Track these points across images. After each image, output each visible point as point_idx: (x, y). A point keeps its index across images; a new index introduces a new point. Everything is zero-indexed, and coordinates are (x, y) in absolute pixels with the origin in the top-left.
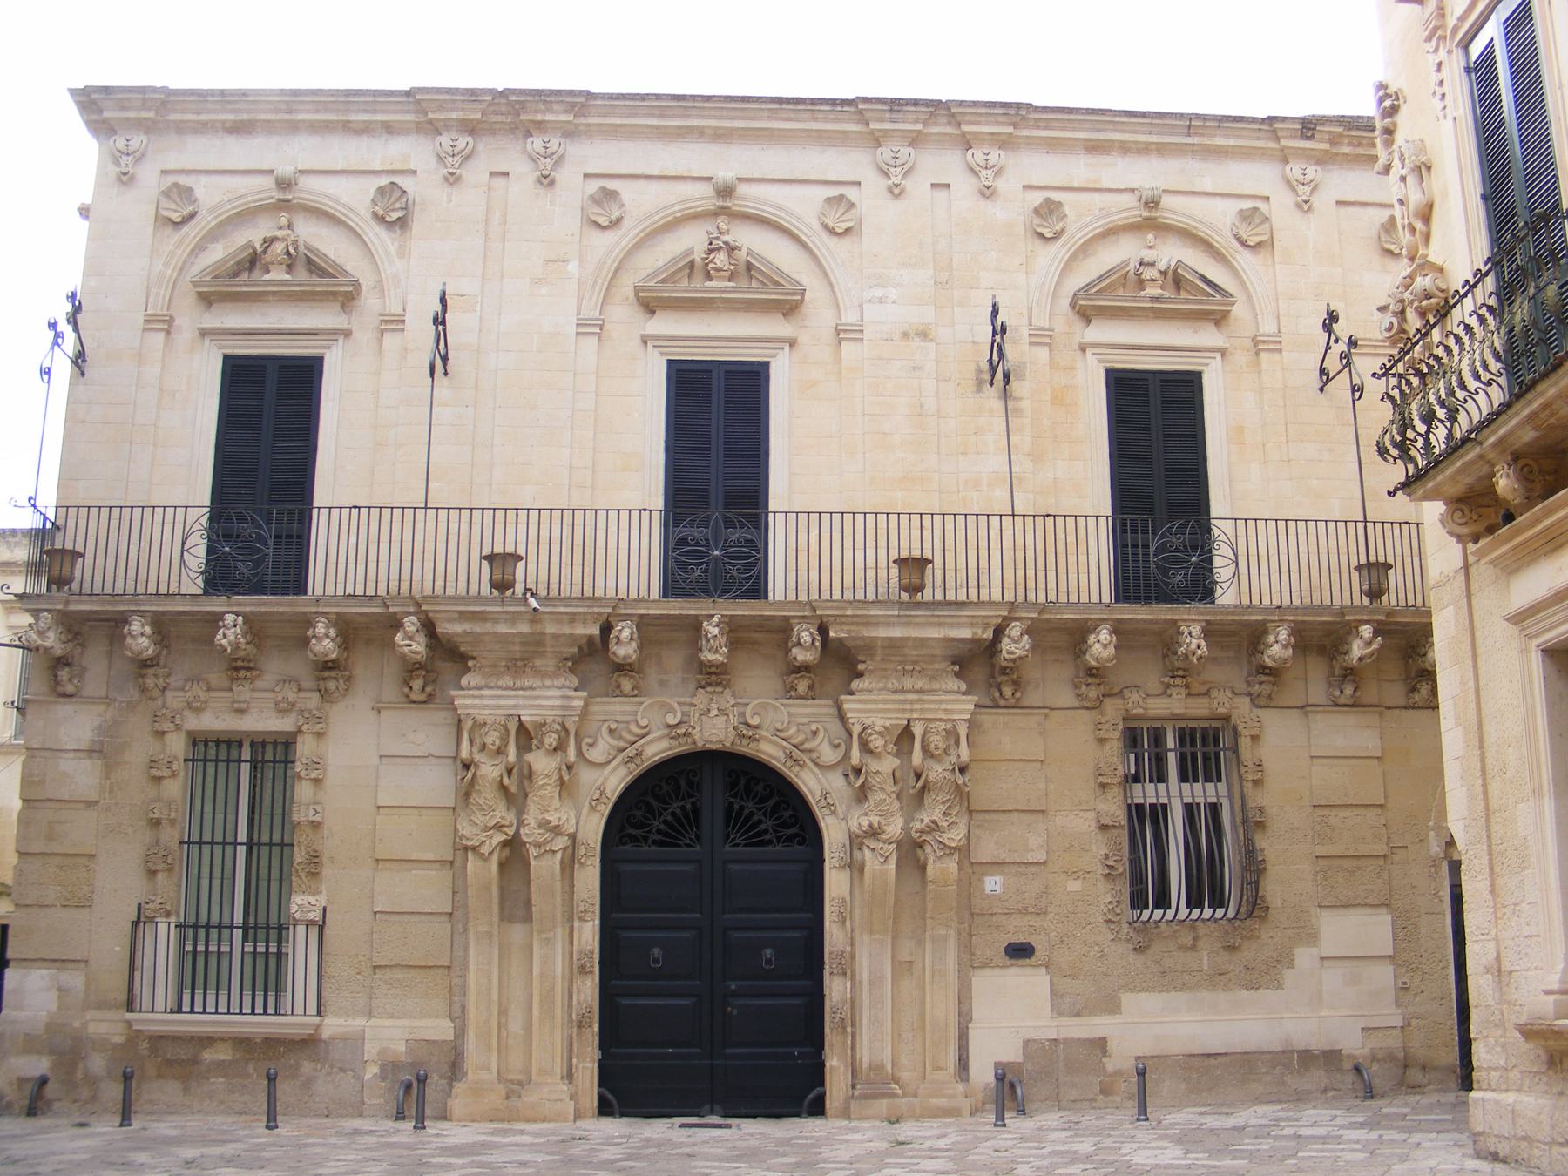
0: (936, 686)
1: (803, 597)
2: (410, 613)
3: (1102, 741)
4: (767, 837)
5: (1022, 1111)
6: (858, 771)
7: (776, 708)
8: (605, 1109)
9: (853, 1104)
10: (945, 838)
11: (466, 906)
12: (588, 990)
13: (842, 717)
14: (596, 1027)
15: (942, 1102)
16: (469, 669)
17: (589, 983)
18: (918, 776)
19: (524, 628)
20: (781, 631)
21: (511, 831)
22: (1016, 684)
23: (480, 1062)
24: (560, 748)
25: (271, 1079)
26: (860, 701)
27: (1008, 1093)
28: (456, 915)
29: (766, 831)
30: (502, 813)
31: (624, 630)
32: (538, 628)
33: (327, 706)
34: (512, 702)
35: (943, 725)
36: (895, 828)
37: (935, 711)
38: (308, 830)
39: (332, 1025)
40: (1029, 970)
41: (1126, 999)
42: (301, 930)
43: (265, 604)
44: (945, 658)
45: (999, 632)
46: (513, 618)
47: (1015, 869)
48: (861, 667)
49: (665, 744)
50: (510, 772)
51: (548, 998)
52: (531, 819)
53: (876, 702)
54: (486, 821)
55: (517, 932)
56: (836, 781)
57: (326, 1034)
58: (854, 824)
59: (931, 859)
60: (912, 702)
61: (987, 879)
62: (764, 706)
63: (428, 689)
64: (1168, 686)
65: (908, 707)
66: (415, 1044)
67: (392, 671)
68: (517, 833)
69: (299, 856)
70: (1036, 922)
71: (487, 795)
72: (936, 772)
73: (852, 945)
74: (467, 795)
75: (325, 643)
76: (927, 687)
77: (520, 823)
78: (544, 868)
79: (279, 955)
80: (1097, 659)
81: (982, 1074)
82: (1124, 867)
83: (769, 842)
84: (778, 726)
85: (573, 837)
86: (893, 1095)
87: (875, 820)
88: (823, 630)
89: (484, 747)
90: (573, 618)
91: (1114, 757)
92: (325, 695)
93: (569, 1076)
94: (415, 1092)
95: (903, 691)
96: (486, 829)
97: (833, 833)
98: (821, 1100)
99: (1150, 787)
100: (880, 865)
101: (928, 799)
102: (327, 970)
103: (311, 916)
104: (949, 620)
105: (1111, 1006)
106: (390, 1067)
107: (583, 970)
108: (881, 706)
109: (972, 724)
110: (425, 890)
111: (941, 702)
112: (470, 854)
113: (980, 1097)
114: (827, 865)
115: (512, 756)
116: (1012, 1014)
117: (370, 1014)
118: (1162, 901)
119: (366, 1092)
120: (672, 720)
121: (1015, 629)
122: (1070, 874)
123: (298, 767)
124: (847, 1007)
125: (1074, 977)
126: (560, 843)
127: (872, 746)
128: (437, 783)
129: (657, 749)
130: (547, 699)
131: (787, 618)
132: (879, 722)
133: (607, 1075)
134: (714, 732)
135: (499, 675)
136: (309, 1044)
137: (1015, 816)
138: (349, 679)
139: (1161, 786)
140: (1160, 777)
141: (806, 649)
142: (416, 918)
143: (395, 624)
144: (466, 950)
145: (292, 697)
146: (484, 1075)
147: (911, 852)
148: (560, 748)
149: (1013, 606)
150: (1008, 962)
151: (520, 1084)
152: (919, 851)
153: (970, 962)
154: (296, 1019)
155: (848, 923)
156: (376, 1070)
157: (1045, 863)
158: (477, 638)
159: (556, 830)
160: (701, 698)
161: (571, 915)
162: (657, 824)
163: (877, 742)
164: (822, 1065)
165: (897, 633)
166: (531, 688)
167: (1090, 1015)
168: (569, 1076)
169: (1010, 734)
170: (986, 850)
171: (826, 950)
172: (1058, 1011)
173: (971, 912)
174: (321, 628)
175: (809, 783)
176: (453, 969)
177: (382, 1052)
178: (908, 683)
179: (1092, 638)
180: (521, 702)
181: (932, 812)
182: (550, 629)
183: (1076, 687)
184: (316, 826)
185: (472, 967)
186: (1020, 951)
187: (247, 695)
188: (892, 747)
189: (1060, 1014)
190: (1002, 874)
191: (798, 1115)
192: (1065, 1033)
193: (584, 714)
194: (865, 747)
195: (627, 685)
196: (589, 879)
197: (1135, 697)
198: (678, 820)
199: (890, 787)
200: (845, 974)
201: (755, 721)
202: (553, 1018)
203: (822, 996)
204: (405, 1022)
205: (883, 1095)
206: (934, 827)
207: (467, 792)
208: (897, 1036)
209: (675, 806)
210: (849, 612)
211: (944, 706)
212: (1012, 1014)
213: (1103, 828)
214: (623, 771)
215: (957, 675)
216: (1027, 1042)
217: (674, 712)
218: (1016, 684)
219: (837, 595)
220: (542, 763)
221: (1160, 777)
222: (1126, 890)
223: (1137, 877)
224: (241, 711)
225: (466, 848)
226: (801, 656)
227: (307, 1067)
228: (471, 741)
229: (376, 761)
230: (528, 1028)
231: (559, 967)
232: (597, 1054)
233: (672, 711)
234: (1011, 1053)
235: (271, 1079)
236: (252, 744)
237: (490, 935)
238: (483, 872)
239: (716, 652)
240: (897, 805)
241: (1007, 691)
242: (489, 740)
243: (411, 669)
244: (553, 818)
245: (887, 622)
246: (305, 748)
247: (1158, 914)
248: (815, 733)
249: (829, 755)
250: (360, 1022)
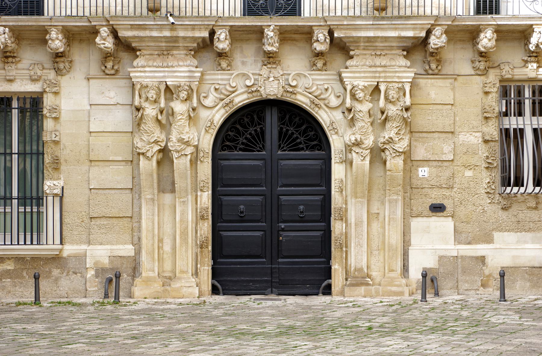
0: (394, 63)
1: (320, 15)
2: (103, 26)
3: (487, 93)
4: (301, 146)
5: (437, 294)
6: (350, 110)
7: (305, 76)
8: (215, 291)
9: (346, 289)
10: (397, 147)
11: (140, 184)
12: (206, 228)
13: (341, 81)
14: (210, 248)
15: (394, 289)
16: (137, 56)
17: (206, 225)
18: (383, 113)
19: (167, 34)
20: (307, 34)
21: (163, 144)
22: (439, 61)
23: (149, 267)
24: (188, 98)
25: (37, 278)
26: (351, 72)
27: (430, 282)
28: (135, 189)
29: (300, 143)
30: (158, 134)
31: (222, 35)
32: (175, 34)
33: (59, 78)
34: (162, 74)
35: (396, 85)
36: (369, 142)
37: (393, 77)
38: (52, 145)
39: (69, 249)
40: (442, 219)
41: (497, 235)
42: (50, 199)
43: (21, 21)
44: (399, 48)
45: (429, 32)
46: (161, 28)
47: (435, 164)
48: (352, 53)
49: (245, 96)
50: (161, 112)
51: (184, 233)
52: (174, 137)
53: (359, 72)
54: (150, 138)
55: (167, 198)
56: (338, 116)
57: (65, 254)
58: (347, 139)
59: (388, 158)
60: (380, 72)
61: (420, 169)
62: (299, 75)
63: (116, 67)
64: (526, 62)
65: (378, 75)
66: (112, 258)
67: (95, 58)
68: (166, 145)
69: (47, 159)
70: (447, 193)
71: (150, 125)
72: (393, 110)
73: (346, 204)
74: (139, 125)
75: (57, 42)
76: (388, 64)
77: (168, 140)
78: (181, 164)
79: (38, 212)
80: (485, 48)
81: (415, 274)
82: (497, 163)
83: (302, 149)
84: (307, 86)
85: (196, 147)
86: (368, 284)
87: (358, 137)
88: (331, 33)
89: (147, 98)
90: (193, 28)
91: (494, 103)
92: (58, 72)
93: (196, 274)
94: (114, 282)
95: (375, 66)
96: (149, 143)
97: (336, 143)
98: (329, 286)
99: (513, 119)
100: (361, 161)
101: (388, 125)
102: (66, 220)
103: (55, 191)
104: (401, 26)
105: (489, 239)
106: (100, 271)
107: (203, 218)
108: (362, 75)
109: (413, 85)
110: (118, 176)
111: (396, 72)
112: (141, 157)
113: (414, 286)
114: (333, 161)
115: (162, 105)
116: (433, 242)
117: (89, 243)
118: (519, 182)
119: (88, 284)
120: (248, 83)
121: (438, 31)
122: (467, 167)
123: (45, 111)
124: (343, 237)
125: (468, 223)
126: (189, 150)
127: (357, 96)
128: (121, 119)
129: (241, 99)
130: (181, 71)
131: (311, 27)
132: (361, 83)
133: (216, 273)
134: (272, 89)
135: (154, 60)
136: (56, 260)
137: (436, 135)
138: (71, 62)
139: (520, 119)
140: (520, 113)
141: (321, 43)
142: (113, 192)
143: (95, 32)
144: (140, 208)
145: (39, 73)
146: (151, 274)
147: (378, 154)
148: (188, 98)
149: (437, 18)
150: (431, 214)
151: (170, 278)
152: (383, 154)
153: (409, 214)
154: (49, 246)
155: (344, 193)
156: (93, 272)
157: (452, 160)
158: (141, 39)
159: (187, 143)
160: (265, 71)
161: (196, 188)
162: (242, 140)
163: (360, 95)
164: (330, 268)
165: (371, 34)
166: (172, 66)
167: (477, 243)
168: (196, 274)
169: (435, 90)
170: (420, 153)
171: (332, 207)
172: (458, 241)
173: (410, 186)
174: (54, 34)
175: (324, 117)
176: (134, 218)
177: (96, 263)
178: (378, 61)
179: (482, 35)
180: (166, 74)
181: (390, 132)
182: (182, 34)
183: (473, 62)
184: (56, 143)
185: (143, 217)
186: (437, 208)
187: (13, 73)
188: (368, 97)
189: (459, 243)
190: (429, 166)
191: (317, 294)
192: (462, 253)
193: (201, 80)
194: (353, 96)
195: (224, 64)
196: (205, 170)
197: (507, 68)
198: (253, 137)
199: (368, 120)
200: (342, 219)
201: (294, 83)
202: (187, 243)
203: (330, 231)
204: (108, 247)
205: (362, 284)
206: (390, 141)
207: (139, 123)
208: (370, 253)
209: (252, 130)
210: (345, 23)
211: (397, 75)
212: (433, 242)
213: (486, 142)
214: (223, 111)
215: (405, 57)
216: (441, 258)
217: (250, 79)
218: (439, 61)
219: (339, 13)
220: (179, 107)
221: (520, 113)
222: (497, 175)
223: (505, 168)
224: (10, 81)
225: (139, 154)
226: (319, 47)
227: (56, 272)
228: (140, 96)
229: (89, 107)
230: (174, 248)
231: (190, 216)
232: (211, 262)
233: (248, 78)
235: (37, 278)
236: (18, 99)
237: (153, 200)
238: (148, 166)
239: (272, 45)
240: (371, 129)
241: (433, 66)
242: (150, 95)
243: (106, 56)
244: (186, 137)
245: (366, 28)
246: (48, 101)
247: (515, 189)
248: (327, 90)
249: (334, 102)
250: (84, 247)
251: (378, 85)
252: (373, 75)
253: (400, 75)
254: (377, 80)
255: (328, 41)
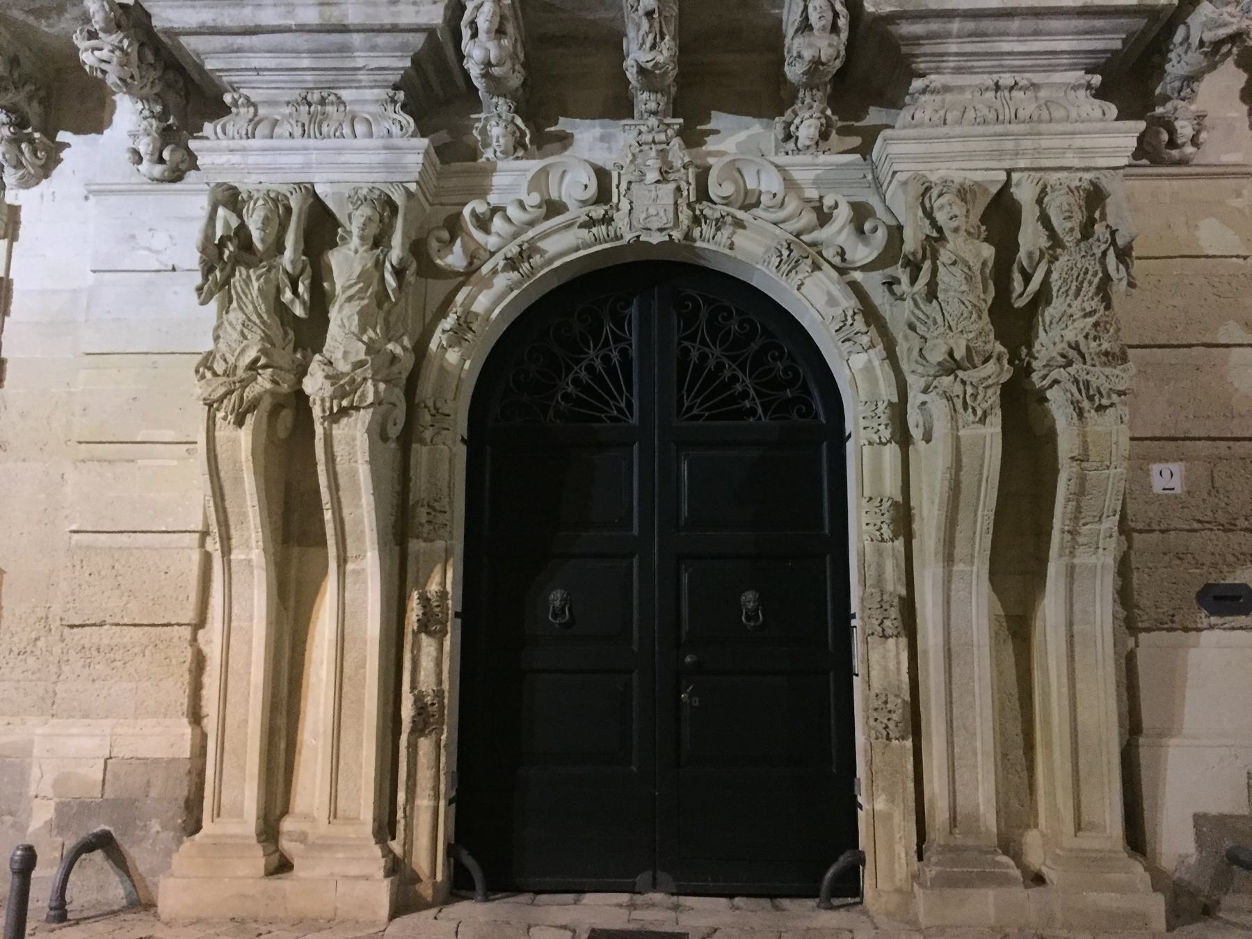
12: (433, 664)
61: (1155, 468)
65: (1009, 145)
108: (957, 146)
198: (598, 378)
211: (1078, 142)
234: (1227, 800)
251: (1008, 184)
252: (995, 145)
253: (1088, 142)
254: (1007, 164)
255: (843, 22)
